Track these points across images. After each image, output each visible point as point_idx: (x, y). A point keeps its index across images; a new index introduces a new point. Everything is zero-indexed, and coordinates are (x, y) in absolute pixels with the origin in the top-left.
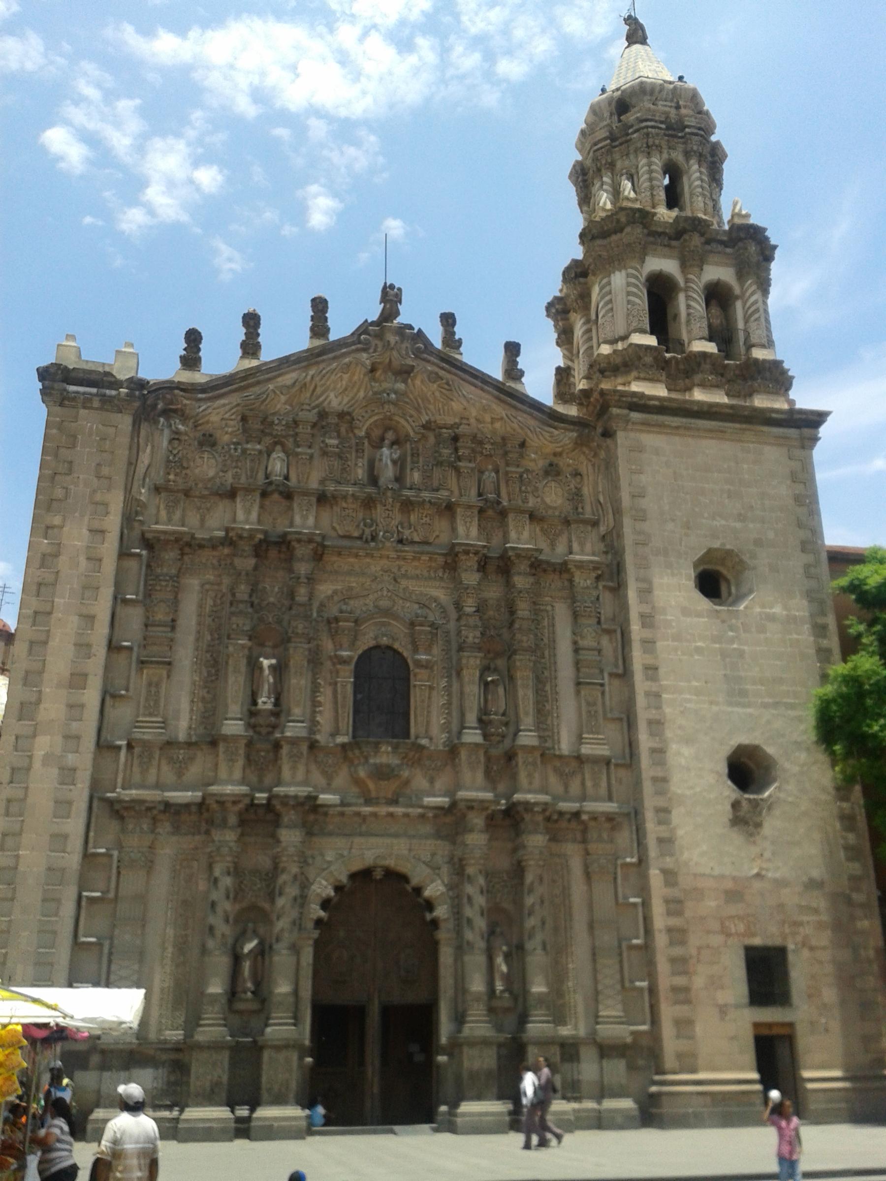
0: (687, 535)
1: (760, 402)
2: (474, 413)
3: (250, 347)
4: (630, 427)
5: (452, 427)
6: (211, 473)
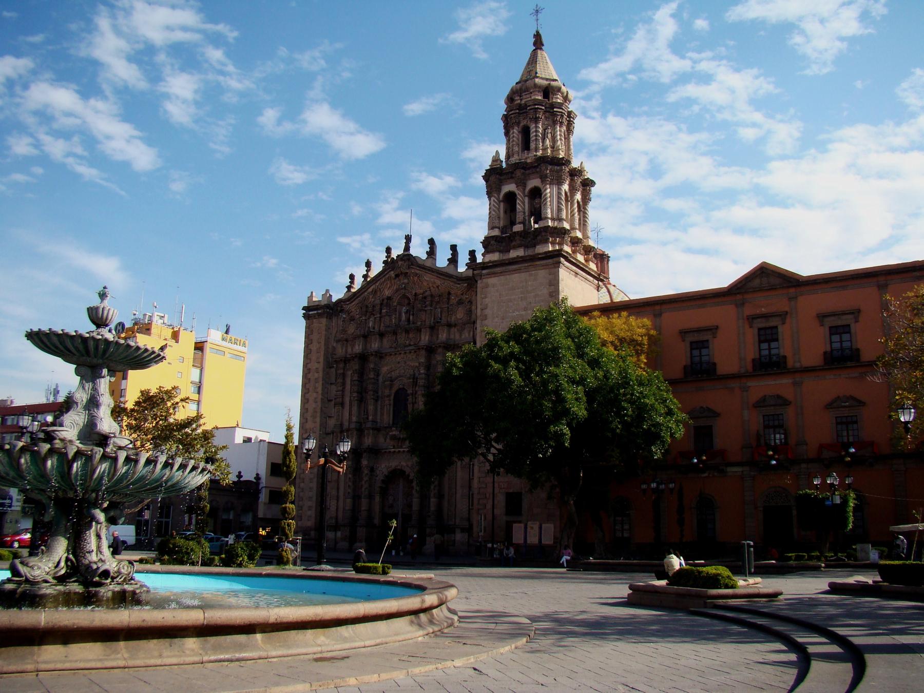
0: (503, 322)
1: (541, 249)
2: (431, 285)
3: (365, 276)
4: (483, 277)
5: (423, 294)
6: (353, 331)
